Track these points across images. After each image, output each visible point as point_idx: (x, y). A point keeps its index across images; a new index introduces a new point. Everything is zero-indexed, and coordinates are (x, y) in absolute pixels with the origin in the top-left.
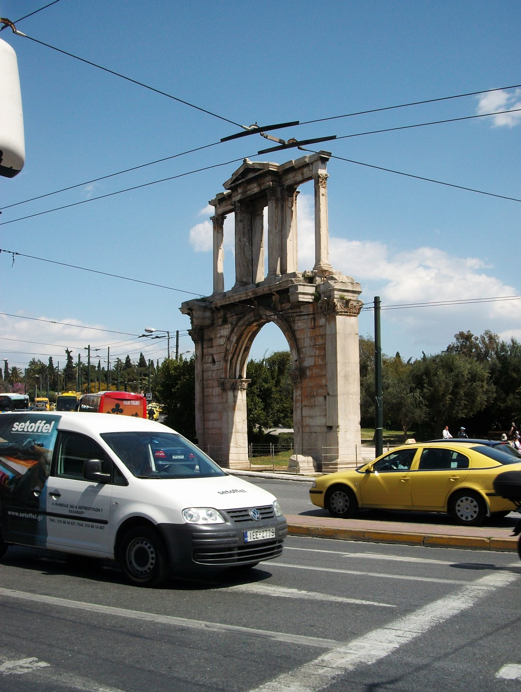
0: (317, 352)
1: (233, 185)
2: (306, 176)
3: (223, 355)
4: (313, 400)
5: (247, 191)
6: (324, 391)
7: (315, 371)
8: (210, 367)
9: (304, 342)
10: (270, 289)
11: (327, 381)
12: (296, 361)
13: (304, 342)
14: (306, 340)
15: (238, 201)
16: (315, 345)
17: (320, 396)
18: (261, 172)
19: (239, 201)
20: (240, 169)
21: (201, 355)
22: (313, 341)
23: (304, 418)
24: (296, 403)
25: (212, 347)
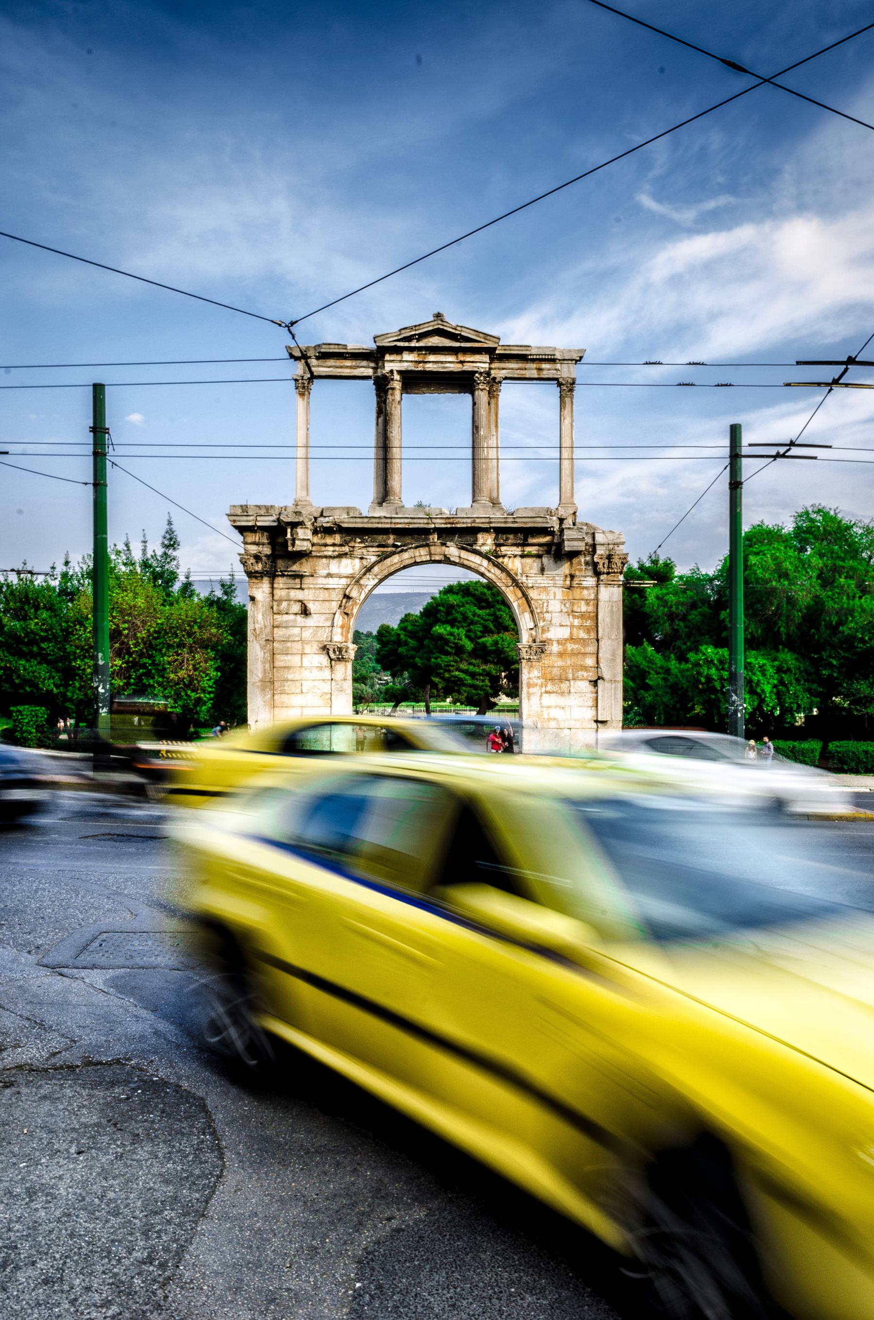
0: (576, 622)
2: (545, 374)
3: (335, 605)
4: (565, 686)
6: (591, 674)
7: (570, 647)
8: (295, 621)
9: (547, 606)
10: (491, 523)
11: (598, 662)
13: (547, 606)
14: (551, 602)
15: (397, 371)
16: (573, 611)
17: (582, 680)
19: (399, 372)
21: (269, 599)
25: (301, 588)
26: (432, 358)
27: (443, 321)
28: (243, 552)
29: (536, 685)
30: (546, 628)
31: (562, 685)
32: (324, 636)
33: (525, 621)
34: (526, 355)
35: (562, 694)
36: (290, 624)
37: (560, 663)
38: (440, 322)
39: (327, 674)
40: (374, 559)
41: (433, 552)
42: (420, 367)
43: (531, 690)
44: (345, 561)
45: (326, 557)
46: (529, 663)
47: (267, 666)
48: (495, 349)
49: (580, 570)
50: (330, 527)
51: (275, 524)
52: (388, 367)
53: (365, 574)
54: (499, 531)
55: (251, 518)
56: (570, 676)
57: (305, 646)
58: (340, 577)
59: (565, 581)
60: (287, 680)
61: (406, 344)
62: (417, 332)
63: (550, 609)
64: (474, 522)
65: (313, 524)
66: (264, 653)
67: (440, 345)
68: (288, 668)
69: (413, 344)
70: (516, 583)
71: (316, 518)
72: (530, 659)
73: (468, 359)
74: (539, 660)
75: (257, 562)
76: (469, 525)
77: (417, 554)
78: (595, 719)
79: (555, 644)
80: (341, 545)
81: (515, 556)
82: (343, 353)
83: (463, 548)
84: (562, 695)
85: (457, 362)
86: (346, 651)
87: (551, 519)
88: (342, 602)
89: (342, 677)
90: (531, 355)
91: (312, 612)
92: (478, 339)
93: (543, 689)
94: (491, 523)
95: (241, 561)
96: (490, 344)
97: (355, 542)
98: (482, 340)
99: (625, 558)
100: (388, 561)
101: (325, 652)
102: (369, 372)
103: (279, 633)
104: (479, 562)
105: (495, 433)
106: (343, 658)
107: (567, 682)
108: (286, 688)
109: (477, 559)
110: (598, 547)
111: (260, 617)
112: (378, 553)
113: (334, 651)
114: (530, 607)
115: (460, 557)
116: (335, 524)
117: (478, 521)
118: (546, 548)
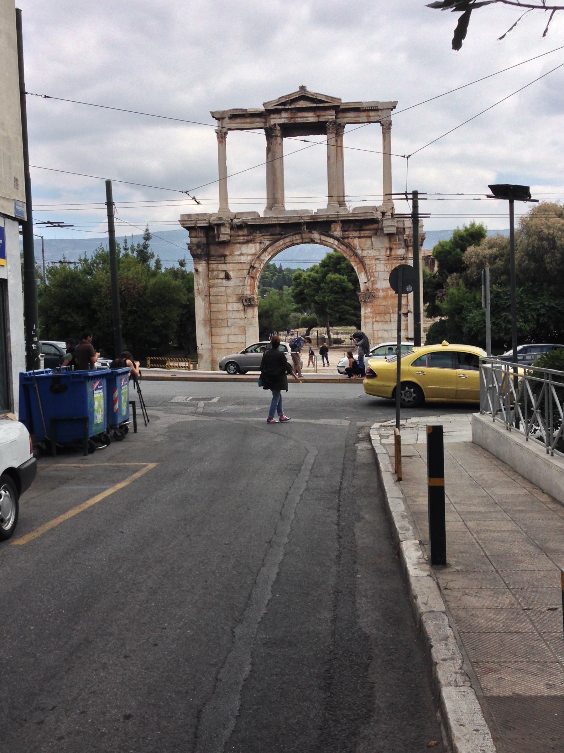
1: (280, 107)
3: (245, 272)
5: (296, 118)
8: (222, 282)
9: (376, 268)
10: (339, 217)
12: (365, 283)
13: (376, 268)
18: (326, 105)
19: (279, 125)
20: (295, 94)
21: (206, 271)
22: (388, 267)
23: (375, 332)
24: (365, 319)
25: (225, 263)
26: (300, 115)
27: (305, 91)
28: (189, 242)
29: (370, 317)
30: (375, 282)
31: (386, 317)
32: (239, 291)
33: (362, 278)
34: (359, 108)
35: (386, 322)
36: (219, 285)
37: (384, 303)
38: (303, 92)
39: (242, 315)
40: (268, 243)
41: (304, 237)
42: (292, 121)
43: (367, 320)
44: (250, 245)
45: (239, 243)
46: (365, 304)
47: (207, 312)
48: (339, 106)
49: (396, 244)
50: (240, 225)
51: (207, 225)
52: (273, 122)
53: (263, 252)
54: (343, 222)
55: (193, 222)
56: (391, 311)
57: (229, 298)
58: (248, 255)
59: (386, 252)
60: (218, 319)
61: (283, 107)
62: (289, 99)
63: (377, 270)
64: (328, 217)
65: (230, 224)
66: (205, 303)
67: (304, 106)
68: (219, 311)
69: (287, 107)
70: (356, 255)
71: (232, 220)
72: (365, 301)
73: (322, 114)
74: (370, 302)
75: (198, 248)
76: (325, 220)
77: (294, 239)
78: (407, 337)
79: (381, 291)
80: (248, 236)
81: (355, 237)
82: (245, 114)
83: (322, 234)
84: (386, 323)
85: (316, 117)
86: (253, 300)
87: (376, 213)
88: (249, 270)
89: (251, 316)
90: (362, 107)
91: (232, 277)
92: (328, 101)
93: (374, 320)
94: (339, 217)
95: (189, 249)
96: (336, 104)
97: (256, 233)
98: (331, 101)
99: (424, 236)
100: (277, 244)
101: (241, 301)
102: (262, 125)
103: (213, 290)
104: (332, 242)
105: (341, 160)
106: (251, 304)
107: (389, 315)
108: (218, 324)
109: (331, 240)
110: (406, 230)
111: (201, 281)
112: (270, 239)
113: (246, 301)
114: (365, 269)
115: (320, 239)
116: (244, 222)
117: (330, 216)
118: (374, 232)
